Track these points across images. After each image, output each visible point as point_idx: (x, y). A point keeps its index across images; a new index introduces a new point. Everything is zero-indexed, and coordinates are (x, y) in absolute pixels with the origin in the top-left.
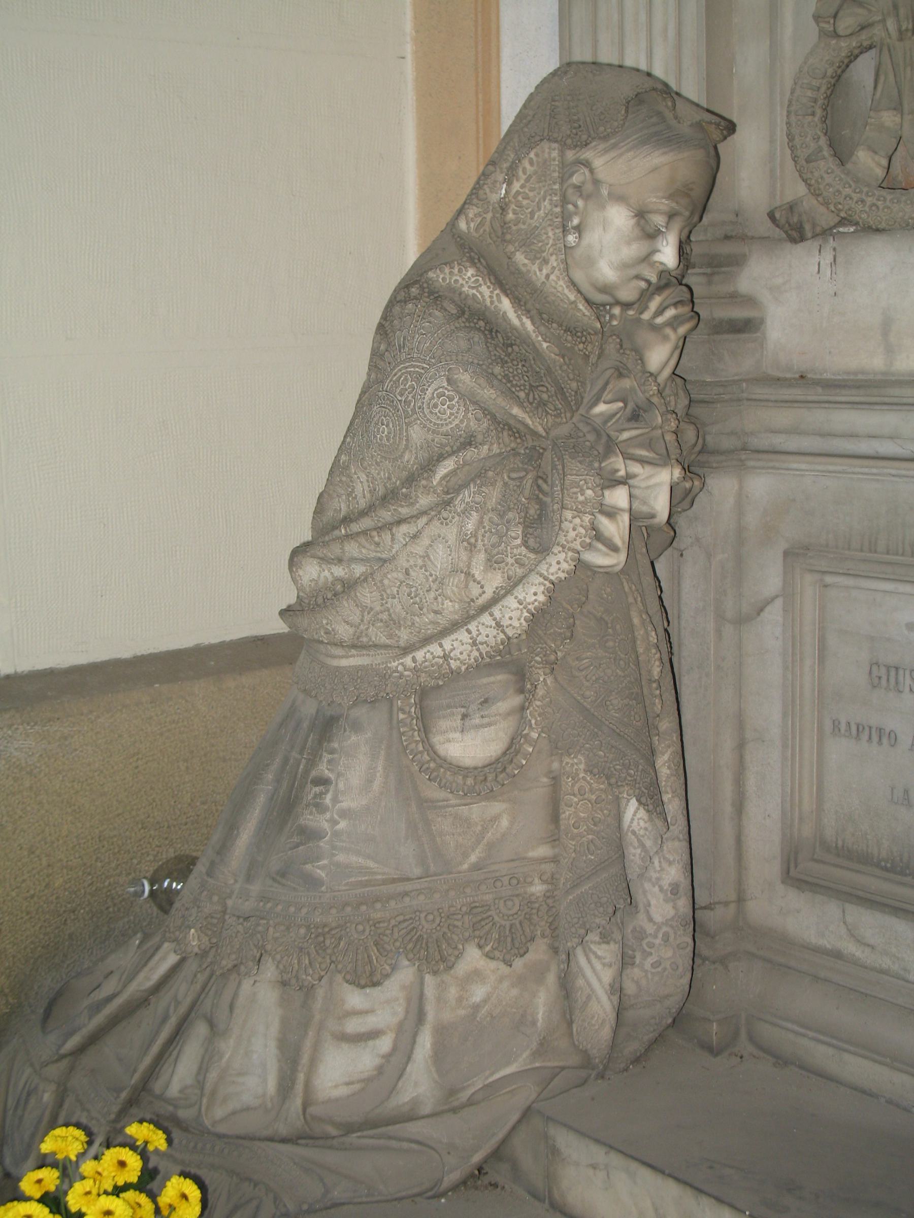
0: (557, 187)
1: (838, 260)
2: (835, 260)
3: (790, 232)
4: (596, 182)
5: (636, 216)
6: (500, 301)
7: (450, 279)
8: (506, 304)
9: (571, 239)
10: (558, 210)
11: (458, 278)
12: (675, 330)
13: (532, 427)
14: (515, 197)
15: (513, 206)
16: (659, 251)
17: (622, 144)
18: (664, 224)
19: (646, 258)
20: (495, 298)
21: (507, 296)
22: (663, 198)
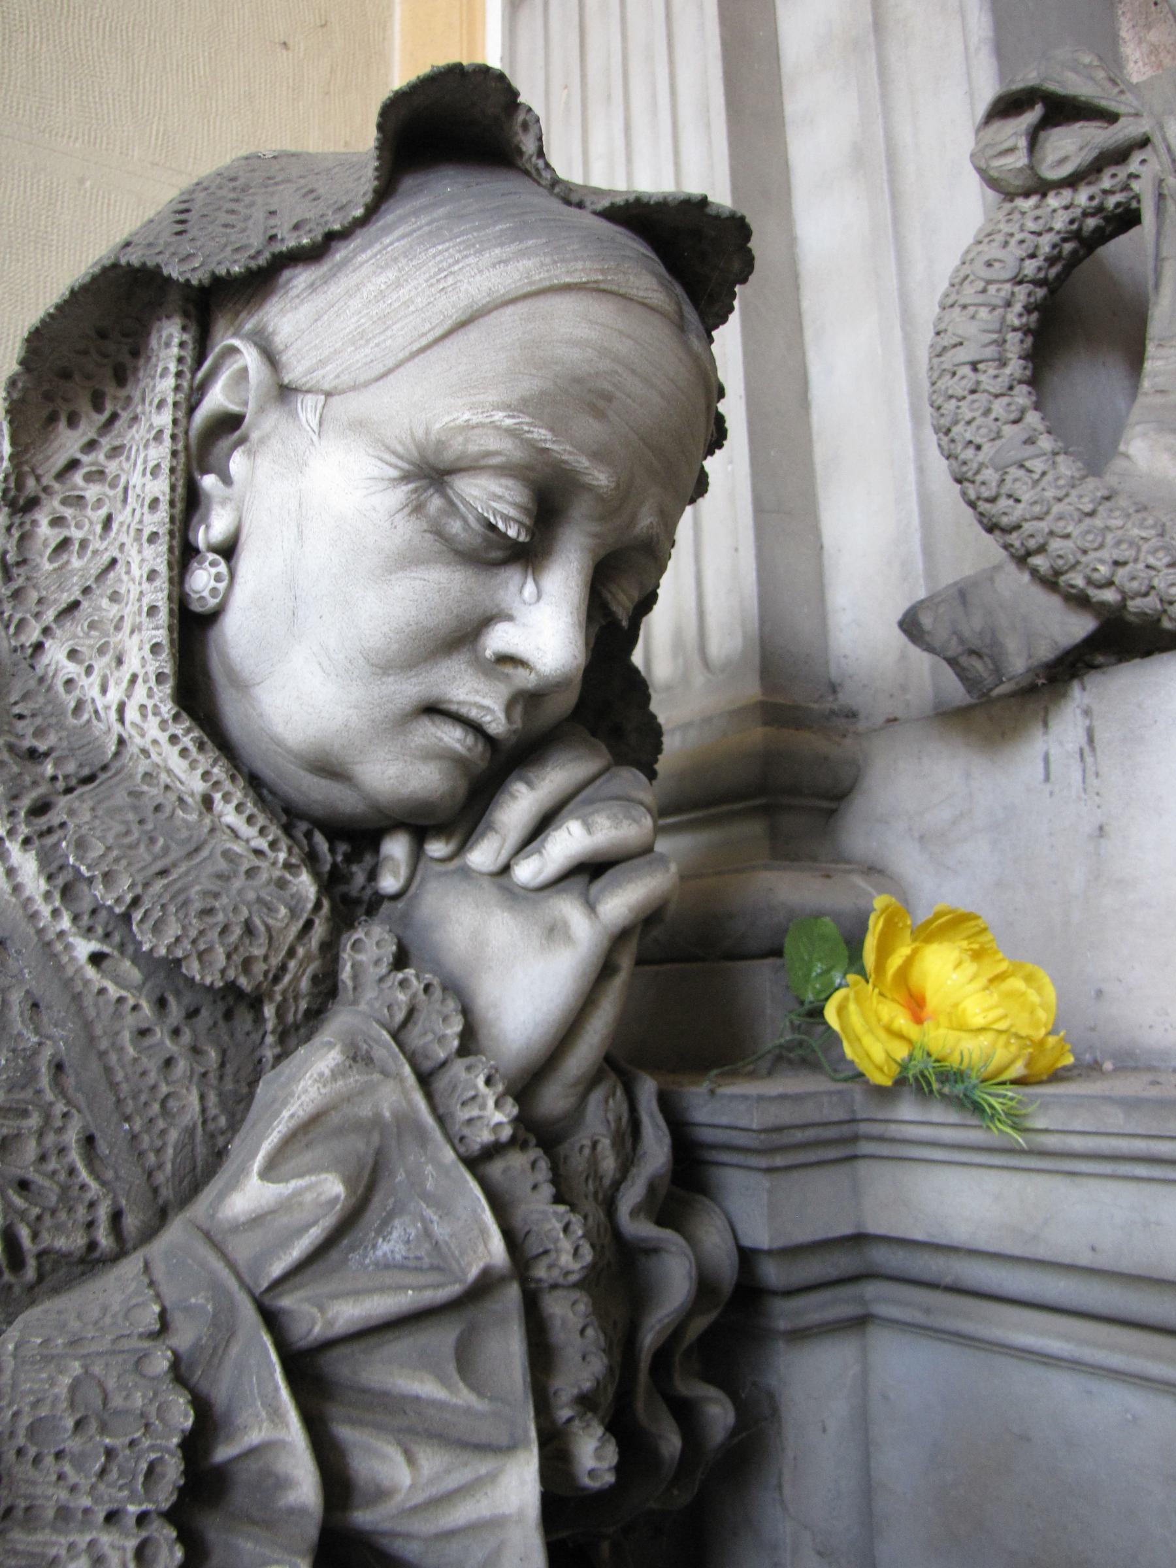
0: (164, 419)
1: (1101, 736)
2: (1091, 740)
3: (964, 660)
4: (285, 393)
5: (406, 478)
9: (203, 580)
10: (160, 487)
12: (591, 907)
14: (61, 475)
15: (53, 505)
16: (509, 618)
17: (363, 257)
18: (512, 512)
22: (497, 408)
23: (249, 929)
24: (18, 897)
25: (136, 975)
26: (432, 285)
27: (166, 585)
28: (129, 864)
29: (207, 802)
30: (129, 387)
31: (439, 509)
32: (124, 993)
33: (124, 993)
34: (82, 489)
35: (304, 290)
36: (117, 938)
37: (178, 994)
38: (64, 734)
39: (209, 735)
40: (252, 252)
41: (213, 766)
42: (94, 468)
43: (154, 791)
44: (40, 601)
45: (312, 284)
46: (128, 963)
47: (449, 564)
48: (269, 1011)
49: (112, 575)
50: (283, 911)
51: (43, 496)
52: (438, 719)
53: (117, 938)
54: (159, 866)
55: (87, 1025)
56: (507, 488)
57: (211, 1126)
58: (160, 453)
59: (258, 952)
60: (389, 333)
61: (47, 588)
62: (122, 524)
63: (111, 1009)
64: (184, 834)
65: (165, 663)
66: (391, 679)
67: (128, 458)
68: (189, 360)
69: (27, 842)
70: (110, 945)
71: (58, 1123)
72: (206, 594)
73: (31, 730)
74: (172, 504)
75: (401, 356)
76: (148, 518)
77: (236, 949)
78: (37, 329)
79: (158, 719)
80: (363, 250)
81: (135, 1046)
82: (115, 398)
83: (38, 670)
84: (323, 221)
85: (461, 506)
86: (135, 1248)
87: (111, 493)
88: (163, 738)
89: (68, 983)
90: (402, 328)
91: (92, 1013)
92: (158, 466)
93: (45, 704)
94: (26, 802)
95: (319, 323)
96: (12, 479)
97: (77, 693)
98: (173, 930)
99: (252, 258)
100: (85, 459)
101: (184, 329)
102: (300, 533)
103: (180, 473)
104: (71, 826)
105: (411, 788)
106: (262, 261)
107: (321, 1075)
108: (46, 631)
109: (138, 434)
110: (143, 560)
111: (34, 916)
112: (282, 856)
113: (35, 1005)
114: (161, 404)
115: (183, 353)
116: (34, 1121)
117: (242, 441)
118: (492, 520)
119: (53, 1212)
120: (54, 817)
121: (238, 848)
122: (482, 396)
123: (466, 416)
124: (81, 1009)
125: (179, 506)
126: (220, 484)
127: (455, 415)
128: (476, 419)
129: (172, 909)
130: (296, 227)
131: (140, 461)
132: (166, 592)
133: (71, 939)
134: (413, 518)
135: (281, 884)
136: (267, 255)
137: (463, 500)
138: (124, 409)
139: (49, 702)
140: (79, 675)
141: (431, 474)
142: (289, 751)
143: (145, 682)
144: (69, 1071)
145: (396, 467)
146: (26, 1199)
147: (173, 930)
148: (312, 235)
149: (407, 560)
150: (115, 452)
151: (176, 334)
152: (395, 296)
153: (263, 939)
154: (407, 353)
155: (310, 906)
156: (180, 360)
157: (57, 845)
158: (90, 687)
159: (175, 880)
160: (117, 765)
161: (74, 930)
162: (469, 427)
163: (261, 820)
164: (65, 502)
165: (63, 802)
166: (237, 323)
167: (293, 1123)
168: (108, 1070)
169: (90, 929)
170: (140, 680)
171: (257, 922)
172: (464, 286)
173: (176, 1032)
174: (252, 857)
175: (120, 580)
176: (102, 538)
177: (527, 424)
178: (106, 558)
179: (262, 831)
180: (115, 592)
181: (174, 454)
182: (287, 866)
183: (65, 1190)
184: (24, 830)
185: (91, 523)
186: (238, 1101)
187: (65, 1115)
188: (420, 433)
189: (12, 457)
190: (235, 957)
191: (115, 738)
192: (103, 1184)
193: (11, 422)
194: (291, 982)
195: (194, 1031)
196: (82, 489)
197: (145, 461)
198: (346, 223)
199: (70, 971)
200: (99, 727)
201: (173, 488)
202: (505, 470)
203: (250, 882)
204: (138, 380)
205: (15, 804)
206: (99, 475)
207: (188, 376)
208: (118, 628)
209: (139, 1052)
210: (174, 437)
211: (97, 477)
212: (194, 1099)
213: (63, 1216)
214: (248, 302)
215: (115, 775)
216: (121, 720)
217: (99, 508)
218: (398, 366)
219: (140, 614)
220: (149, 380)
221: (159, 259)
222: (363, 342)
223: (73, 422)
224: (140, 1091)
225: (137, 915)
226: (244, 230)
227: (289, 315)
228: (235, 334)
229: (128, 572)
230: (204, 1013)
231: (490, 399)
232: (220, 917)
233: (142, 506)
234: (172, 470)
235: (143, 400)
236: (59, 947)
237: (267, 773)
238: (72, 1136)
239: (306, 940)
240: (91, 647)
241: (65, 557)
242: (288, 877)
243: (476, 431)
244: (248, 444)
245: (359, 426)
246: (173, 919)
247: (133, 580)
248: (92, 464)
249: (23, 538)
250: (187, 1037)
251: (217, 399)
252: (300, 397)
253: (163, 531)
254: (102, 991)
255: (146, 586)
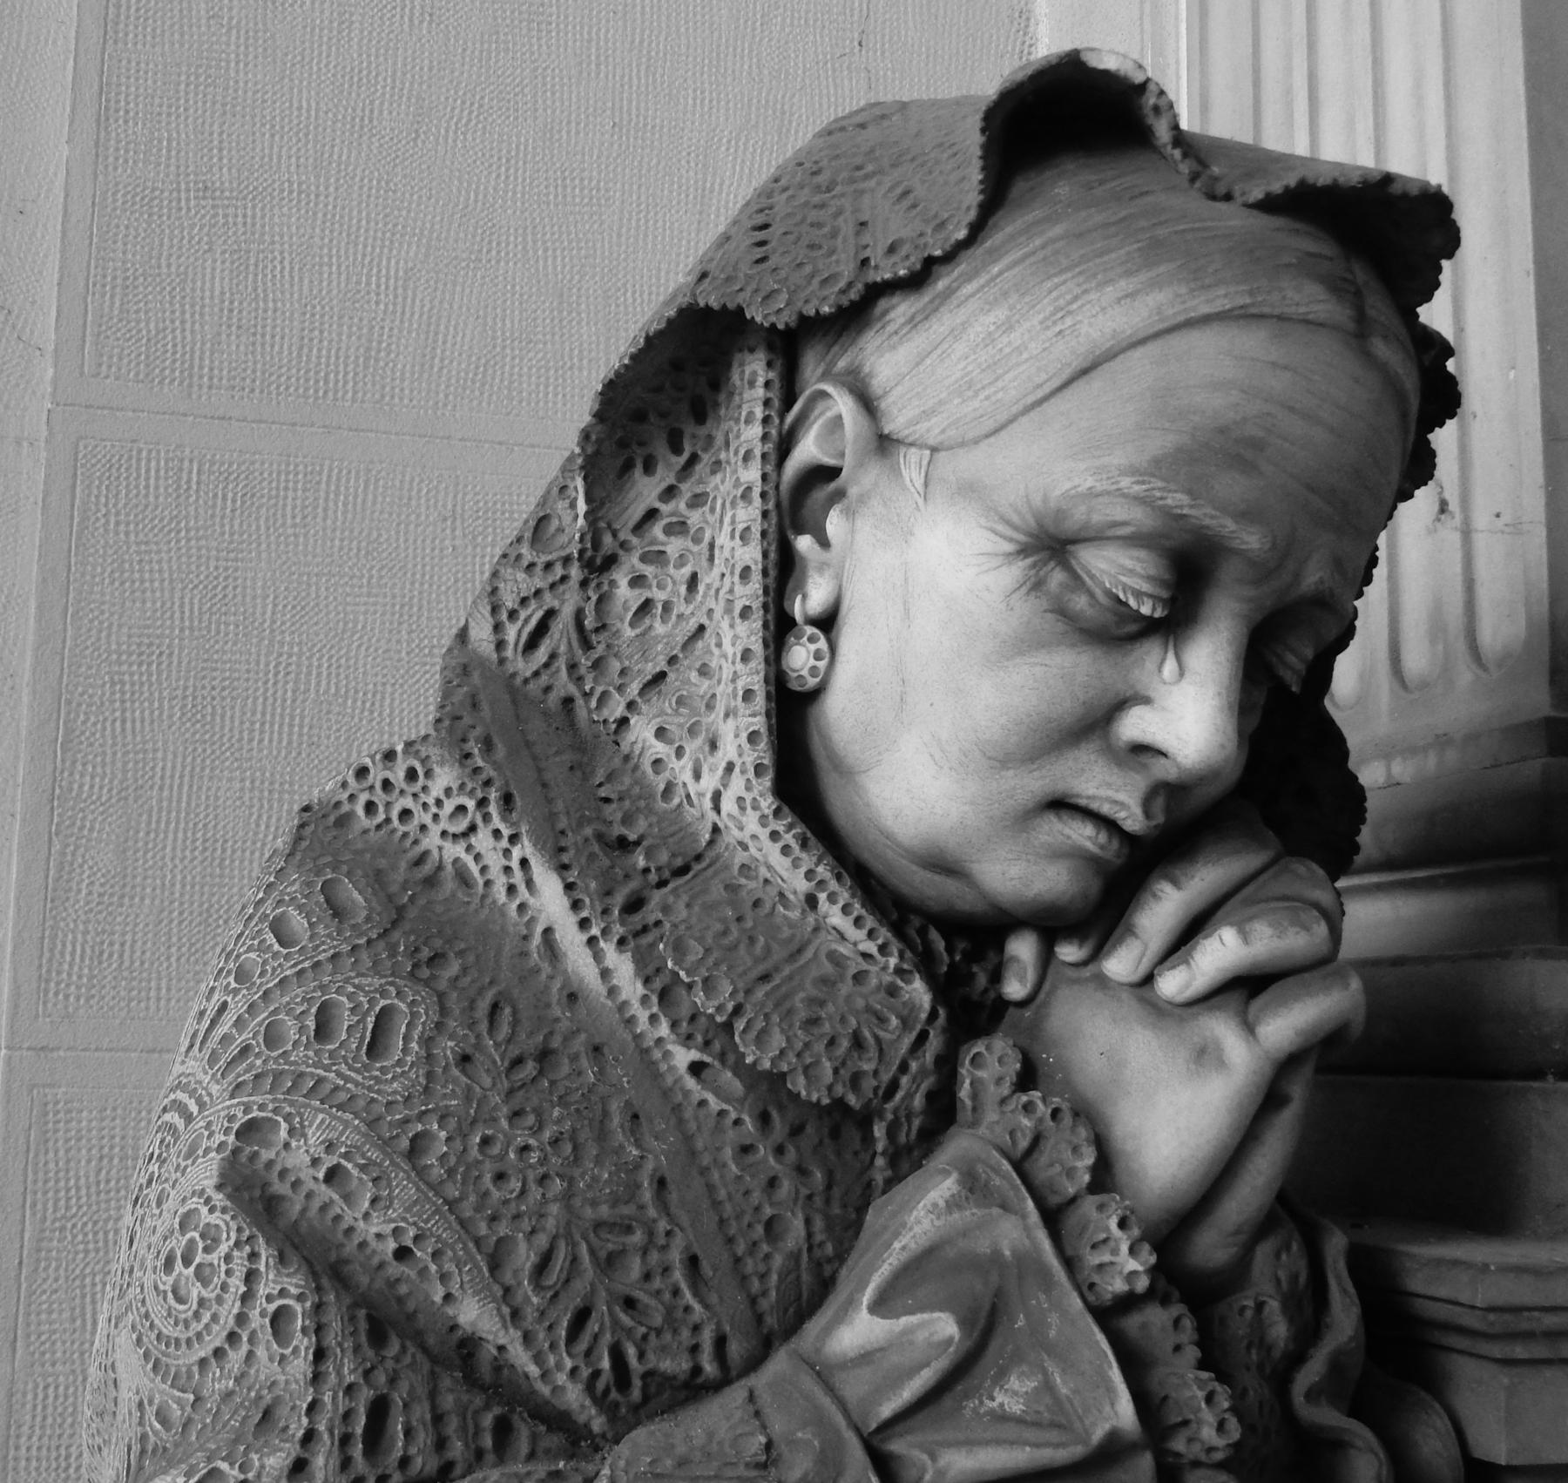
4: (884, 444)
5: (1023, 551)
6: (529, 883)
7: (388, 805)
8: (550, 898)
9: (801, 657)
10: (751, 554)
11: (408, 802)
13: (545, 1390)
15: (632, 562)
17: (969, 289)
18: (1145, 587)
19: (1094, 724)
20: (518, 877)
21: (563, 868)
23: (858, 1043)
24: (613, 1001)
25: (737, 1087)
26: (1048, 328)
27: (762, 666)
28: (730, 968)
29: (811, 901)
30: (709, 423)
31: (1061, 584)
32: (725, 1107)
33: (725, 1107)
34: (663, 544)
35: (903, 325)
36: (717, 1046)
37: (781, 1108)
38: (654, 819)
39: (813, 833)
40: (842, 284)
41: (817, 865)
42: (674, 519)
43: (752, 885)
44: (623, 672)
45: (912, 318)
46: (729, 1074)
47: (1073, 645)
48: (879, 1131)
49: (700, 644)
50: (894, 1021)
51: (621, 552)
52: (1065, 815)
53: (717, 1046)
54: (761, 969)
55: (688, 1139)
56: (1138, 559)
57: (817, 1253)
58: (749, 514)
59: (868, 1067)
60: (1000, 384)
61: (630, 657)
62: (708, 586)
63: (711, 1123)
64: (786, 933)
65: (763, 753)
66: (1011, 773)
67: (713, 510)
68: (776, 403)
69: (622, 942)
70: (710, 1055)
71: (662, 1241)
72: (805, 673)
73: (619, 815)
74: (765, 573)
75: (1014, 410)
76: (739, 589)
77: (844, 1063)
78: (611, 381)
79: (758, 813)
80: (969, 280)
81: (737, 1165)
82: (694, 436)
83: (623, 745)
84: (922, 241)
85: (1087, 579)
86: (740, 1376)
87: (695, 549)
88: (764, 834)
89: (666, 1093)
90: (1015, 378)
91: (693, 1126)
92: (748, 529)
93: (632, 785)
94: (619, 899)
95: (921, 368)
96: (588, 537)
97: (667, 775)
98: (777, 1040)
99: (843, 292)
100: (665, 508)
101: (769, 365)
102: (907, 611)
103: (772, 535)
104: (667, 926)
105: (1035, 891)
106: (854, 295)
107: (935, 1205)
108: (631, 705)
109: (721, 486)
110: (736, 637)
111: (631, 1021)
112: (893, 961)
113: (636, 1116)
114: (747, 457)
115: (770, 395)
116: (638, 1237)
117: (840, 495)
118: (1122, 596)
119: (659, 1332)
120: (651, 913)
121: (843, 949)
122: (1106, 460)
123: (1089, 484)
124: (681, 1121)
125: (772, 573)
126: (816, 547)
127: (1076, 481)
128: (1099, 487)
129: (776, 1018)
130: (892, 249)
131: (727, 520)
132: (762, 674)
133: (670, 1047)
134: (1032, 597)
135: (892, 991)
136: (860, 286)
137: (1088, 573)
138: (705, 450)
139: (636, 783)
140: (668, 756)
141: (1050, 545)
142: (899, 845)
143: (743, 772)
144: (671, 1187)
145: (1011, 540)
146: (633, 1318)
147: (777, 1040)
148: (907, 264)
149: (1026, 644)
150: (697, 501)
151: (761, 372)
152: (1005, 339)
153: (873, 1052)
154: (1020, 406)
155: (924, 1016)
156: (767, 403)
157: (653, 945)
158: (682, 771)
159: (778, 986)
160: (711, 854)
161: (673, 1037)
162: (1092, 494)
163: (870, 922)
164: (644, 558)
165: (657, 897)
166: (829, 357)
167: (904, 1256)
168: (711, 1188)
169: (689, 1037)
170: (737, 770)
171: (867, 1034)
172: (1084, 329)
173: (779, 1151)
174: (860, 959)
175: (712, 653)
176: (687, 601)
177: (1159, 489)
178: (692, 625)
179: (871, 934)
180: (704, 665)
181: (765, 514)
182: (899, 971)
183: (669, 1311)
184: (618, 930)
185: (674, 583)
186: (846, 1223)
187: (668, 1234)
188: (1037, 501)
189: (586, 516)
190: (842, 1072)
191: (709, 827)
192: (706, 1306)
193: (585, 478)
194: (903, 1099)
195: (798, 1149)
196: (663, 544)
197: (733, 522)
198: (948, 247)
199: (669, 1080)
200: (690, 813)
201: (765, 555)
202: (1137, 540)
203: (859, 988)
204: (718, 419)
205: (609, 900)
206: (678, 528)
207: (777, 421)
208: (710, 707)
209: (742, 1170)
210: (763, 495)
211: (678, 528)
212: (798, 1224)
213: (668, 1337)
214: (840, 335)
215: (709, 866)
216: (717, 809)
217: (682, 565)
218: (1011, 421)
219: (735, 696)
220: (732, 423)
221: (741, 299)
222: (970, 393)
223: (649, 468)
224: (743, 1212)
225: (740, 1025)
226: (832, 252)
227: (887, 355)
228: (825, 376)
229: (719, 645)
230: (809, 1129)
231: (1116, 462)
232: (827, 1028)
233: (732, 573)
234: (764, 534)
235: (727, 444)
236: (657, 1055)
237: (877, 866)
238: (676, 1256)
239: (920, 1053)
240: (681, 726)
241: (647, 621)
242: (900, 983)
243: (1100, 499)
244: (846, 501)
245: (969, 490)
246: (777, 1030)
247: (725, 656)
248: (672, 514)
249: (600, 600)
250: (791, 1154)
251: (808, 450)
252: (902, 450)
253: (756, 605)
254: (703, 1103)
255: (739, 666)
